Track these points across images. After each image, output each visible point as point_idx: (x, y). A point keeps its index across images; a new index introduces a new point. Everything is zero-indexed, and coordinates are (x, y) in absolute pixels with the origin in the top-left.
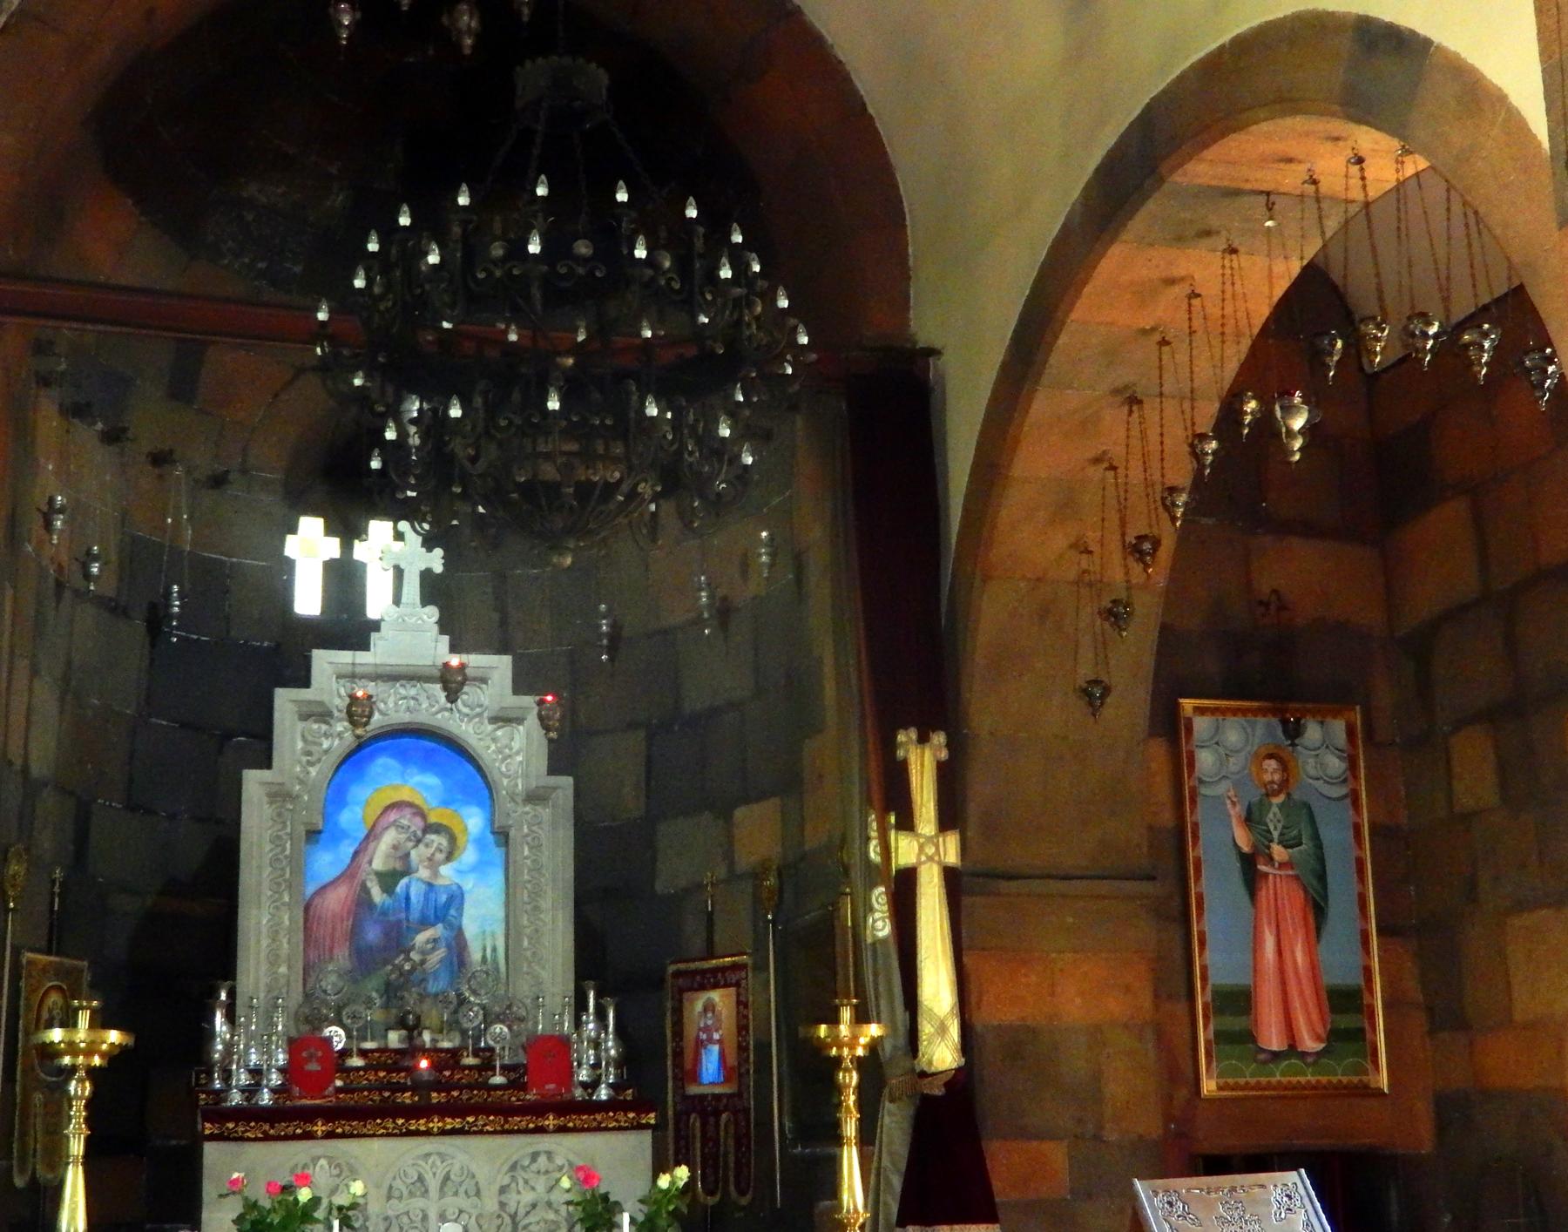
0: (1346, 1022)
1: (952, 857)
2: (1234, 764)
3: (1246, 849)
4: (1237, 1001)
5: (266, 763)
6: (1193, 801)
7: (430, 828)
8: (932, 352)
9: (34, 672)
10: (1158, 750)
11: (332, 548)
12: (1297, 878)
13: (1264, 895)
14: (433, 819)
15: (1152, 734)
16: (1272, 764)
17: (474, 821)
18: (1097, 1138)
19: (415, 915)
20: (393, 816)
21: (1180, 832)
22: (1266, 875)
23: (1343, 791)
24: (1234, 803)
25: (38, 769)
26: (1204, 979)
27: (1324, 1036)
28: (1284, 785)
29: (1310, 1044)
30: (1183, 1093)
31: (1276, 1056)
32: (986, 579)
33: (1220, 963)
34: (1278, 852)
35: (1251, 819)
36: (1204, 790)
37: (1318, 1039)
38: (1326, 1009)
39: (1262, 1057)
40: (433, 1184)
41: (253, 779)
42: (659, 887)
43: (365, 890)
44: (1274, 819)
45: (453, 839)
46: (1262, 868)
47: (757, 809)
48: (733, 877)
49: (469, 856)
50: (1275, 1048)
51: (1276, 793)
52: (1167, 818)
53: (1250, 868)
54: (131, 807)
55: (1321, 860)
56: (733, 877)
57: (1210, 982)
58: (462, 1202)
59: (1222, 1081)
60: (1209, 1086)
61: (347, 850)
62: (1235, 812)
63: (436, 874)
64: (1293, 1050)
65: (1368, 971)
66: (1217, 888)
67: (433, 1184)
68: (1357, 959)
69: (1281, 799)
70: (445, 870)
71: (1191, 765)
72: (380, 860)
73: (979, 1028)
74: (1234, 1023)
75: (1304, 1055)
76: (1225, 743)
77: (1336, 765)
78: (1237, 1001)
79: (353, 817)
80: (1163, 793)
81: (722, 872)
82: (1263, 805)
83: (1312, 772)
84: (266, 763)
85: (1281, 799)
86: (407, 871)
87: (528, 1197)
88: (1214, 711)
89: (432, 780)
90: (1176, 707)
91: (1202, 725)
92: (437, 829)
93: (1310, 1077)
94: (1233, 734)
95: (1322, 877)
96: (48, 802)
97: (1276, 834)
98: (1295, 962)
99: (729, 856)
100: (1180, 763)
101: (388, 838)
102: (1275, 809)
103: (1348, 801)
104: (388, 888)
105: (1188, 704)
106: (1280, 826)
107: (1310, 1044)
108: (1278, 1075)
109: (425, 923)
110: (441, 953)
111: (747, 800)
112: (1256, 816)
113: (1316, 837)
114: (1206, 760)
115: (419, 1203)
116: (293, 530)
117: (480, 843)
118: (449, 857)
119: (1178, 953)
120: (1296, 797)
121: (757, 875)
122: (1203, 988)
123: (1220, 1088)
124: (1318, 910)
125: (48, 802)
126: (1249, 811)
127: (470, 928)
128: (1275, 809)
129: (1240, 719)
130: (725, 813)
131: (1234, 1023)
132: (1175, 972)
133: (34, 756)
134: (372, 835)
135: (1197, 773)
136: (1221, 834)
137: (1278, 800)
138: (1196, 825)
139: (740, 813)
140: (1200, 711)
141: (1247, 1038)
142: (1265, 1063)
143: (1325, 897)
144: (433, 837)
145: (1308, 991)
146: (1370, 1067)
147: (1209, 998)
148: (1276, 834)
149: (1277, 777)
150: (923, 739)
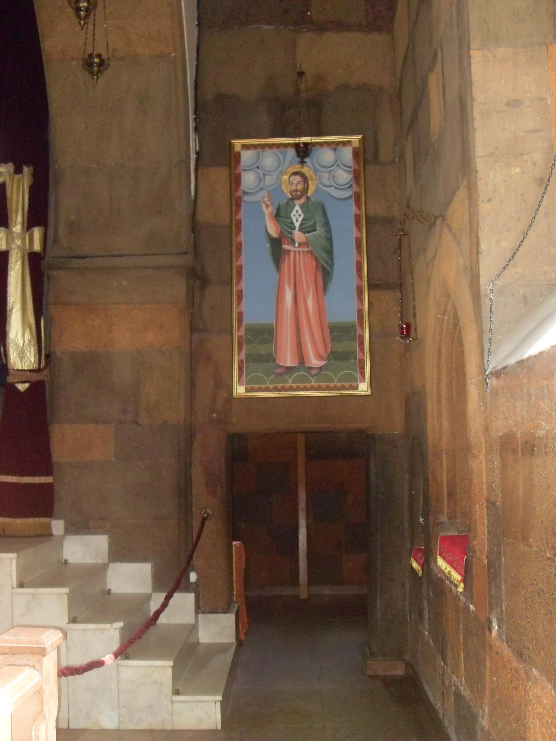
0: (340, 347)
1: (37, 247)
3: (274, 235)
4: (265, 334)
10: (218, 175)
12: (311, 252)
16: (298, 178)
18: (136, 423)
22: (289, 251)
23: (349, 193)
24: (267, 206)
26: (240, 320)
27: (325, 355)
29: (315, 362)
30: (223, 394)
31: (289, 370)
33: (254, 309)
34: (298, 236)
35: (281, 215)
36: (246, 198)
37: (321, 358)
38: (328, 339)
39: (279, 370)
44: (297, 216)
46: (285, 247)
50: (289, 364)
51: (299, 198)
55: (330, 240)
57: (245, 322)
59: (249, 386)
60: (240, 390)
62: (268, 212)
65: (360, 313)
66: (253, 259)
69: (303, 200)
73: (58, 353)
74: (262, 350)
75: (310, 368)
77: (344, 176)
78: (265, 334)
82: (289, 206)
83: (327, 182)
85: (303, 200)
91: (247, 157)
94: (269, 159)
95: (330, 252)
97: (297, 225)
98: (307, 310)
102: (297, 208)
103: (352, 200)
105: (238, 143)
106: (300, 219)
107: (315, 362)
112: (282, 213)
113: (327, 225)
114: (248, 179)
122: (239, 326)
123: (247, 391)
124: (325, 274)
126: (278, 210)
128: (297, 208)
129: (275, 150)
135: (242, 187)
136: (258, 225)
140: (245, 147)
141: (270, 358)
142: (280, 374)
143: (332, 266)
146: (358, 376)
147: (243, 332)
148: (297, 225)
149: (300, 187)
150: (18, 170)
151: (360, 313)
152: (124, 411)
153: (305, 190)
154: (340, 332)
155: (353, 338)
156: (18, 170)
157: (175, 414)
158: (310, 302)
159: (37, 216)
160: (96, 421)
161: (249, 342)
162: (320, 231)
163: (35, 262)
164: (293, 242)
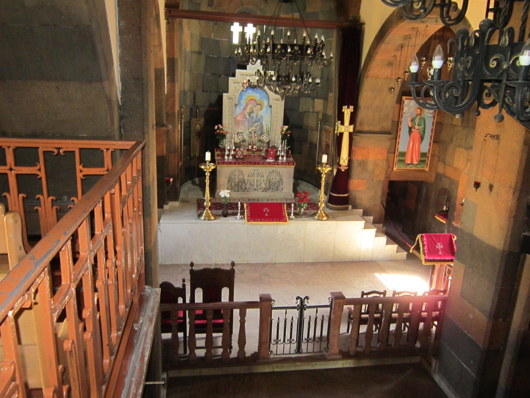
0: (422, 159)
2: (411, 110)
4: (403, 154)
5: (227, 92)
6: (402, 117)
7: (257, 104)
8: (364, 24)
9: (185, 71)
10: (398, 106)
11: (240, 29)
13: (412, 134)
14: (258, 103)
15: (397, 103)
16: (419, 110)
17: (265, 103)
18: (373, 180)
19: (254, 120)
20: (251, 102)
21: (398, 122)
23: (432, 115)
25: (186, 90)
28: (420, 114)
29: (415, 162)
30: (390, 170)
31: (408, 164)
32: (367, 77)
34: (416, 127)
35: (413, 120)
36: (404, 115)
40: (256, 175)
41: (225, 95)
42: (300, 110)
43: (245, 115)
44: (417, 121)
45: (261, 107)
47: (319, 100)
48: (313, 112)
49: (264, 109)
52: (396, 119)
53: (410, 129)
54: (203, 91)
55: (425, 129)
56: (313, 112)
58: (260, 178)
60: (395, 169)
61: (242, 107)
62: (409, 119)
63: (258, 113)
64: (412, 163)
67: (256, 175)
68: (428, 147)
70: (260, 112)
71: (403, 110)
72: (248, 110)
74: (401, 158)
76: (410, 105)
79: (243, 102)
80: (397, 115)
81: (311, 110)
82: (415, 118)
84: (227, 92)
86: (253, 112)
87: (272, 177)
88: (409, 99)
89: (258, 95)
90: (401, 99)
91: (406, 102)
92: (259, 104)
93: (414, 168)
95: (424, 132)
96: (188, 94)
99: (313, 107)
100: (401, 109)
101: (249, 107)
104: (250, 116)
107: (415, 162)
108: (408, 168)
109: (256, 122)
110: (259, 127)
111: (317, 98)
113: (425, 124)
114: (405, 109)
115: (253, 178)
116: (233, 25)
117: (266, 107)
118: (261, 110)
119: (394, 145)
120: (422, 116)
121: (318, 113)
125: (188, 94)
127: (264, 123)
130: (313, 99)
131: (401, 158)
132: (393, 150)
133: (185, 87)
134: (247, 105)
137: (418, 117)
138: (401, 122)
139: (316, 100)
140: (406, 99)
144: (258, 106)
145: (417, 154)
151: (429, 150)
152: (370, 177)
153: (420, 114)
154: (424, 155)
155: (426, 157)
156: (348, 107)
157: (382, 178)
158: (417, 146)
159: (352, 121)
160: (362, 179)
161: (399, 156)
162: (423, 126)
163: (351, 134)
164: (415, 128)
